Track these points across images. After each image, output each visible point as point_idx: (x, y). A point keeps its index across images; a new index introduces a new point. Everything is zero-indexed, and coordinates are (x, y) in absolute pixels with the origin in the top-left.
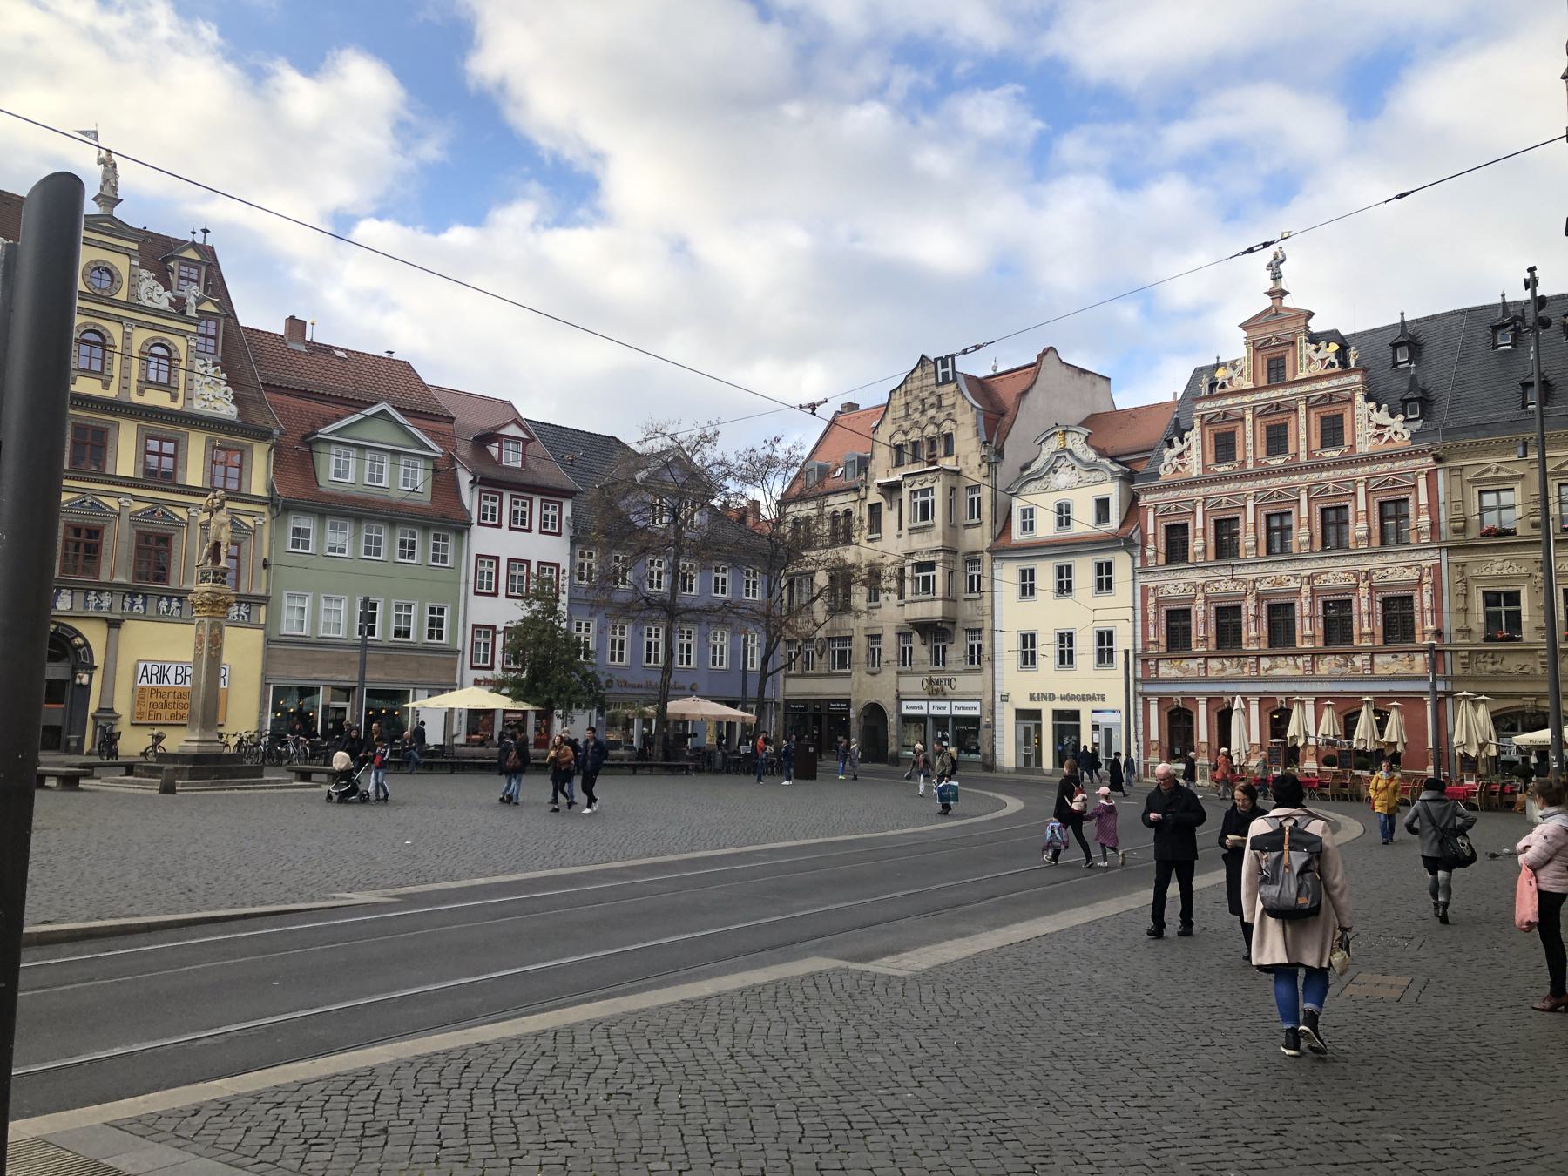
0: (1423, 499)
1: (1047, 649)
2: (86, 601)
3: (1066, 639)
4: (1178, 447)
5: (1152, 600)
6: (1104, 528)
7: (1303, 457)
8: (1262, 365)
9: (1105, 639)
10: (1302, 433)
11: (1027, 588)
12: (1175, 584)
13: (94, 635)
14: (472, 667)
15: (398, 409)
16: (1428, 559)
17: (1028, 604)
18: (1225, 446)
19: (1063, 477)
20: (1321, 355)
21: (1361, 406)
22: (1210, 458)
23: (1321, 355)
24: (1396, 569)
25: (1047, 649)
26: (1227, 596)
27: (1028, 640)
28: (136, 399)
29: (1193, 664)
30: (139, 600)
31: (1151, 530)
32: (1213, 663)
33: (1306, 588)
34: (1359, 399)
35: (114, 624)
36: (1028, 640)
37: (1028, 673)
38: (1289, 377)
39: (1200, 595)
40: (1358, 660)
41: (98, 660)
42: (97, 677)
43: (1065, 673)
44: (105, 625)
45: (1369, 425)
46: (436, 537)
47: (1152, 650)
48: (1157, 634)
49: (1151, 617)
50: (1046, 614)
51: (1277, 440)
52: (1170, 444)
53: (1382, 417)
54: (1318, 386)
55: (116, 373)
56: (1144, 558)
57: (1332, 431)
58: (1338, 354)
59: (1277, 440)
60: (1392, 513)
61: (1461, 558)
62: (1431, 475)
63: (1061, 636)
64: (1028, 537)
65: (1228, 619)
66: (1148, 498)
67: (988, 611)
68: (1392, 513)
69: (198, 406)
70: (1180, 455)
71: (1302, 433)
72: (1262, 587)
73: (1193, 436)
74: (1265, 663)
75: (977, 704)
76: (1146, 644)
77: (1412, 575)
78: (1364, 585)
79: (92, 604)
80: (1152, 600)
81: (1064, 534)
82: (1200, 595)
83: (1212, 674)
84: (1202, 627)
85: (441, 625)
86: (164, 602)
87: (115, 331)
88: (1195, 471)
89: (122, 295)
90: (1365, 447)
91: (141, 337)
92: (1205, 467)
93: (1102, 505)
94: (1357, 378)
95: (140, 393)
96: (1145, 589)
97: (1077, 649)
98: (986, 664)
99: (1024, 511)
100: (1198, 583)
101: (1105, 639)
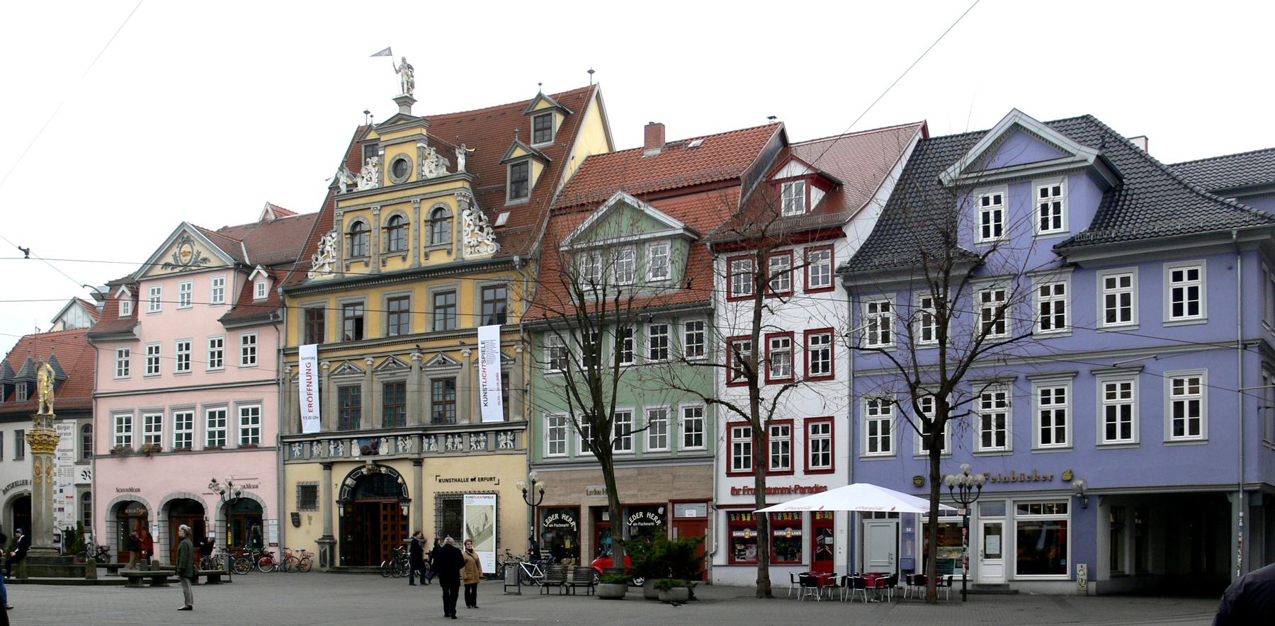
2: (396, 446)
13: (406, 472)
14: (729, 474)
15: (638, 196)
28: (425, 264)
30: (433, 441)
35: (418, 462)
41: (411, 496)
42: (412, 506)
44: (411, 464)
46: (689, 327)
55: (411, 247)
69: (468, 256)
79: (400, 448)
85: (699, 429)
86: (450, 440)
87: (408, 212)
89: (413, 179)
91: (427, 208)
95: (427, 255)
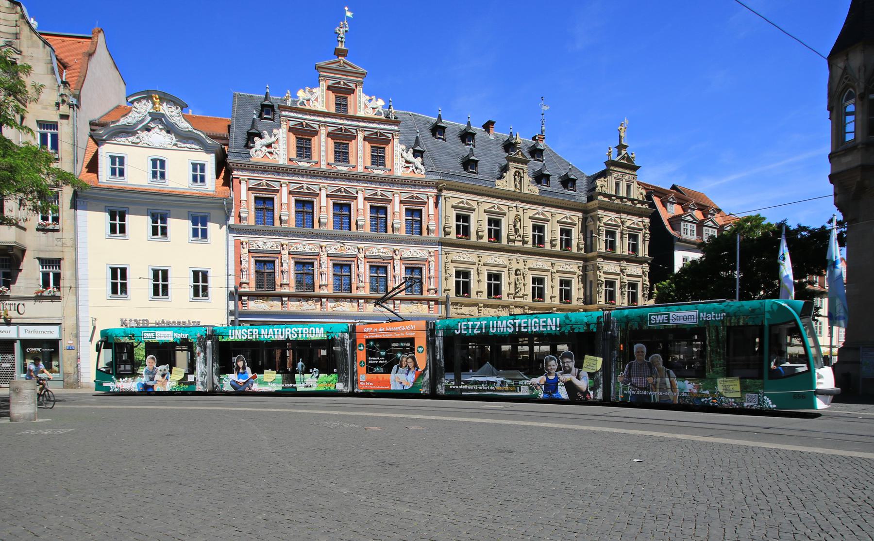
4: (267, 140)
6: (198, 189)
20: (373, 104)
22: (293, 155)
33: (361, 256)
39: (285, 252)
54: (371, 125)
61: (447, 249)
63: (156, 273)
64: (117, 182)
66: (240, 173)
67: (69, 243)
70: (269, 146)
73: (282, 133)
75: (57, 328)
81: (158, 185)
88: (281, 159)
97: (171, 283)
98: (64, 292)
99: (113, 159)
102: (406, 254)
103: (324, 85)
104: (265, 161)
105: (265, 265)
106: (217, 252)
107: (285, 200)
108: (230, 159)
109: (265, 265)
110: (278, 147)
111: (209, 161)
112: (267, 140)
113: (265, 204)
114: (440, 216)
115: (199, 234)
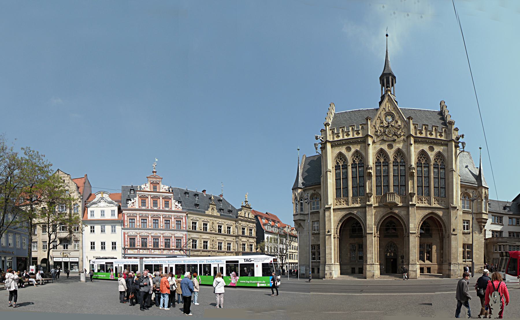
0: (184, 221)
1: (98, 245)
3: (103, 244)
4: (133, 201)
5: (126, 236)
7: (161, 208)
8: (152, 186)
9: (114, 244)
10: (161, 203)
11: (92, 231)
12: (132, 233)
16: (186, 233)
17: (92, 235)
18: (144, 203)
19: (102, 204)
21: (173, 201)
22: (140, 205)
23: (165, 187)
24: (179, 234)
25: (98, 245)
26: (144, 236)
27: (93, 244)
29: (136, 251)
31: (126, 219)
32: (141, 251)
33: (162, 236)
34: (172, 199)
36: (93, 244)
37: (93, 251)
38: (158, 191)
39: (138, 235)
40: (171, 251)
43: (103, 251)
45: (174, 205)
47: (126, 247)
48: (128, 243)
49: (126, 240)
50: (98, 237)
51: (155, 204)
52: (131, 200)
53: (177, 203)
56: (124, 225)
57: (167, 204)
58: (168, 188)
59: (155, 204)
60: (179, 222)
61: (189, 233)
62: (185, 217)
65: (144, 241)
68: (179, 222)
71: (161, 203)
72: (153, 235)
73: (137, 199)
74: (153, 251)
76: (125, 245)
77: (182, 235)
78: (173, 236)
80: (126, 236)
82: (138, 235)
83: (141, 253)
84: (138, 243)
88: (137, 207)
90: (174, 209)
92: (139, 207)
93: (113, 211)
94: (172, 194)
96: (124, 233)
100: (138, 233)
101: (114, 244)
102: (176, 235)
103: (149, 183)
104: (132, 208)
105: (132, 240)
106: (118, 236)
107: (138, 219)
108: (122, 208)
109: (132, 240)
110: (135, 203)
111: (116, 209)
112: (133, 201)
113: (132, 220)
114: (187, 222)
115: (113, 231)
